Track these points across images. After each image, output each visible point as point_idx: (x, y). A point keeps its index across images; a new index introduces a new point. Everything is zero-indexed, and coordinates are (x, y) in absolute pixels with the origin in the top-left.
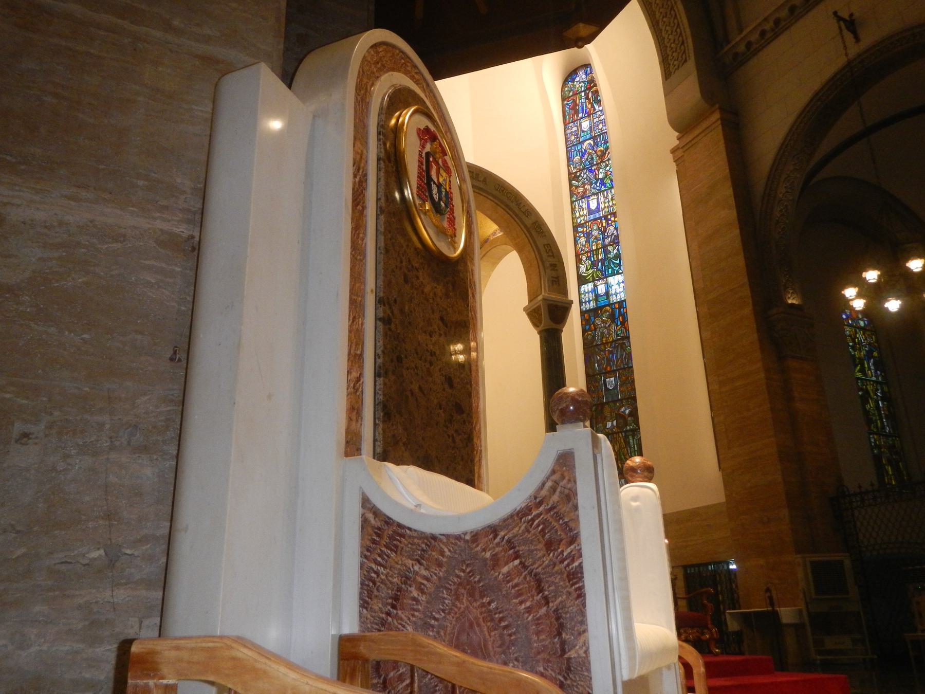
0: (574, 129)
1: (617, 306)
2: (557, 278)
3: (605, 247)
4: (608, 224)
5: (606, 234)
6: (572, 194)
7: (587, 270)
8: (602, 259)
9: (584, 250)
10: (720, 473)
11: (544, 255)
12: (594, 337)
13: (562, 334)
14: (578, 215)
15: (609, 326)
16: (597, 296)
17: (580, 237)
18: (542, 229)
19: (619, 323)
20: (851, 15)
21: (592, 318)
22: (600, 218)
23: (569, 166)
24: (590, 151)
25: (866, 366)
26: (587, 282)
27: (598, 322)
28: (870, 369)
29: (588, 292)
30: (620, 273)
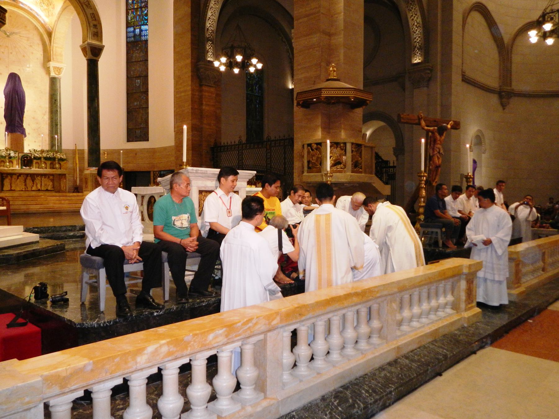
1: (144, 42)
2: (97, 32)
7: (131, 19)
8: (139, 15)
9: (131, 7)
10: (174, 133)
11: (90, 20)
12: (132, 57)
13: (99, 62)
15: (140, 52)
16: (135, 36)
18: (89, 4)
25: (254, 87)
26: (131, 27)
28: (256, 89)
29: (131, 32)
30: (147, 25)
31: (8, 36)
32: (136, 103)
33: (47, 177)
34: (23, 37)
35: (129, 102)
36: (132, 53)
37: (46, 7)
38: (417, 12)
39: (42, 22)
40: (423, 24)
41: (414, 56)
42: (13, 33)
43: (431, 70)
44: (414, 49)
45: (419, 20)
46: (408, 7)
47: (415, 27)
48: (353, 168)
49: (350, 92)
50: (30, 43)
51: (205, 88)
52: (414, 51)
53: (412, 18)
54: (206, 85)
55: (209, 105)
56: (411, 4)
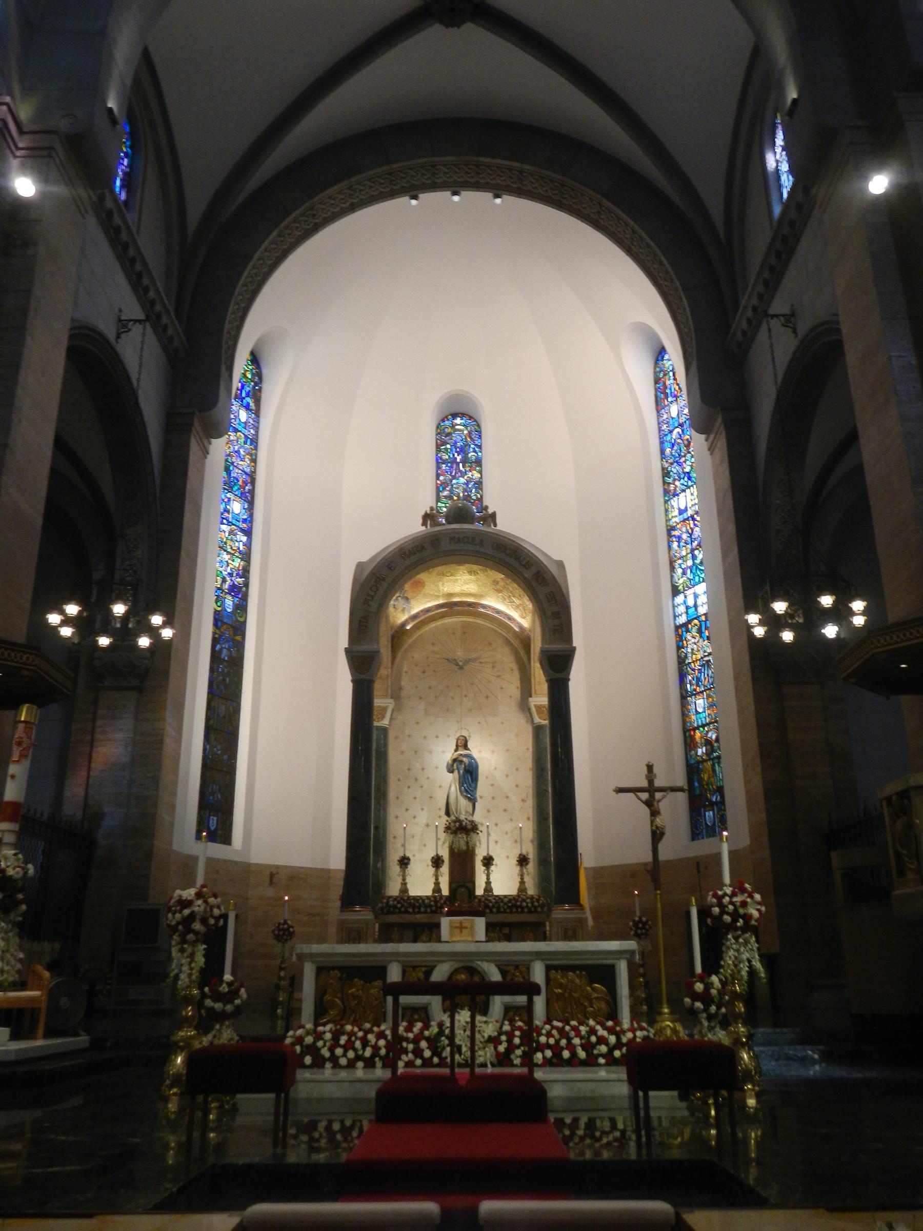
0: (665, 416)
1: (703, 618)
2: (561, 625)
3: (692, 551)
4: (695, 525)
5: (693, 537)
6: (666, 492)
8: (691, 567)
9: (675, 556)
12: (686, 654)
14: (670, 517)
17: (672, 542)
19: (705, 638)
20: (792, 305)
21: (684, 633)
22: (687, 519)
23: (662, 460)
24: (679, 441)
27: (689, 638)
31: (461, 668)
32: (700, 752)
33: (498, 928)
34: (485, 663)
36: (685, 645)
37: (517, 602)
39: (517, 629)
42: (469, 659)
50: (498, 671)
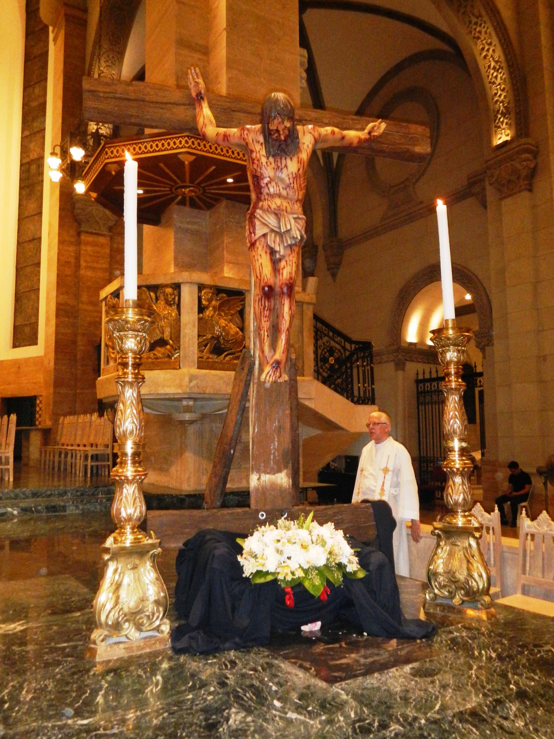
35: (19, 282)
38: (490, 37)
40: (507, 61)
41: (496, 131)
43: (535, 154)
44: (496, 116)
45: (499, 54)
46: (471, 32)
47: (492, 71)
48: (206, 354)
49: (177, 142)
51: (83, 237)
52: (495, 121)
53: (484, 53)
54: (87, 232)
55: (94, 269)
56: (476, 23)
